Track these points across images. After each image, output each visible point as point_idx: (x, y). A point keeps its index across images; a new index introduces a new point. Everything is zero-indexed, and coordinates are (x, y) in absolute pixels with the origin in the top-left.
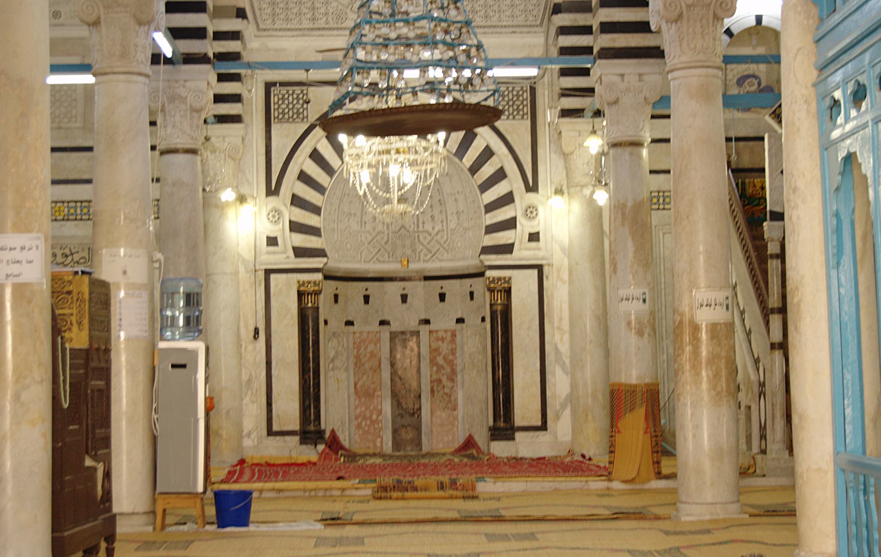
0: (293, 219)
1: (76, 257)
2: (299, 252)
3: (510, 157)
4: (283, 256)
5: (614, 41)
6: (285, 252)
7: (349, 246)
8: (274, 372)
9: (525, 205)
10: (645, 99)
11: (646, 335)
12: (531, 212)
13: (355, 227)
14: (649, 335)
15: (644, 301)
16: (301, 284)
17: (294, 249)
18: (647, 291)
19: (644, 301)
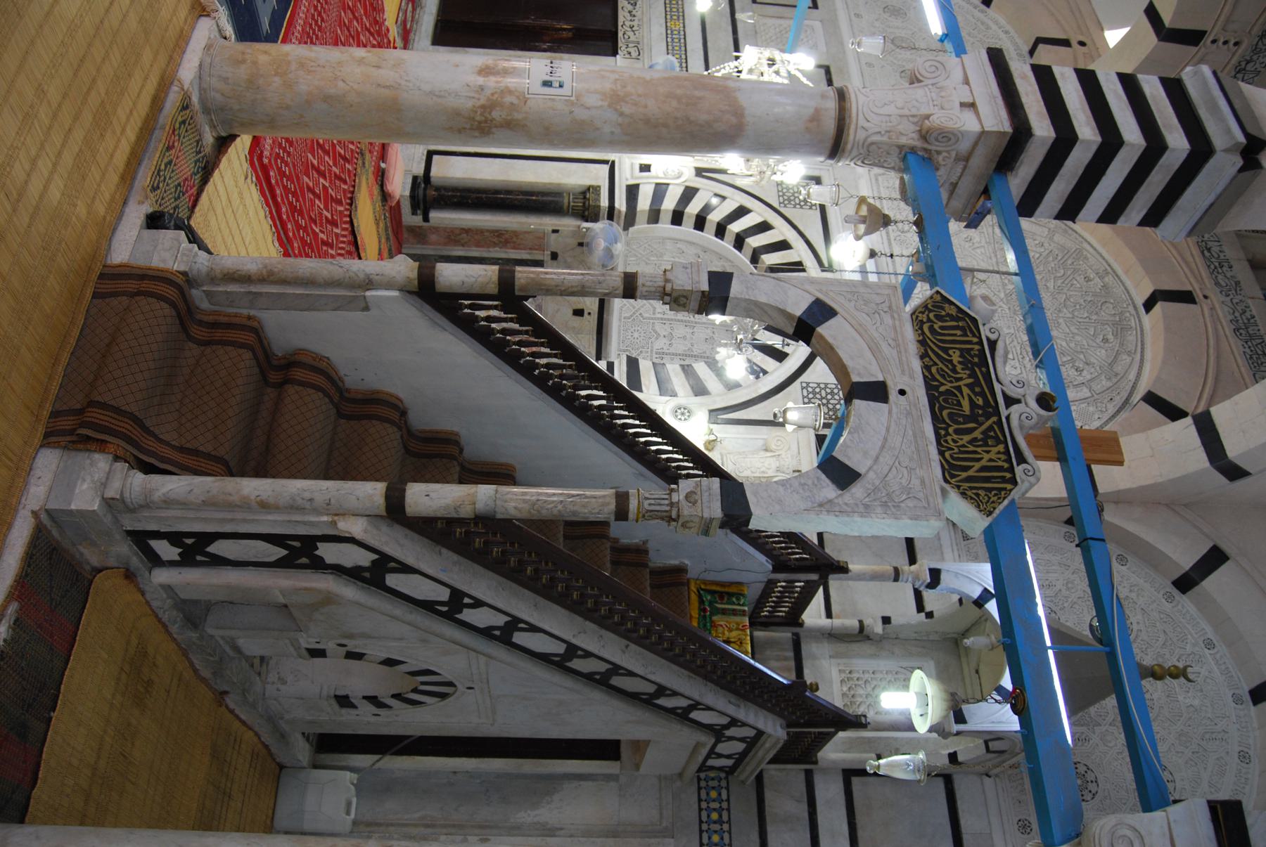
0: (670, 187)
1: (631, 34)
2: (633, 191)
3: (754, 395)
4: (628, 176)
5: (1024, 77)
6: (632, 177)
7: (636, 335)
8: (498, 160)
9: (691, 407)
10: (928, 117)
11: (481, 80)
12: (683, 414)
13: (660, 344)
14: (482, 88)
15: (547, 84)
16: (596, 189)
17: (636, 187)
18: (566, 91)
19: (547, 84)
